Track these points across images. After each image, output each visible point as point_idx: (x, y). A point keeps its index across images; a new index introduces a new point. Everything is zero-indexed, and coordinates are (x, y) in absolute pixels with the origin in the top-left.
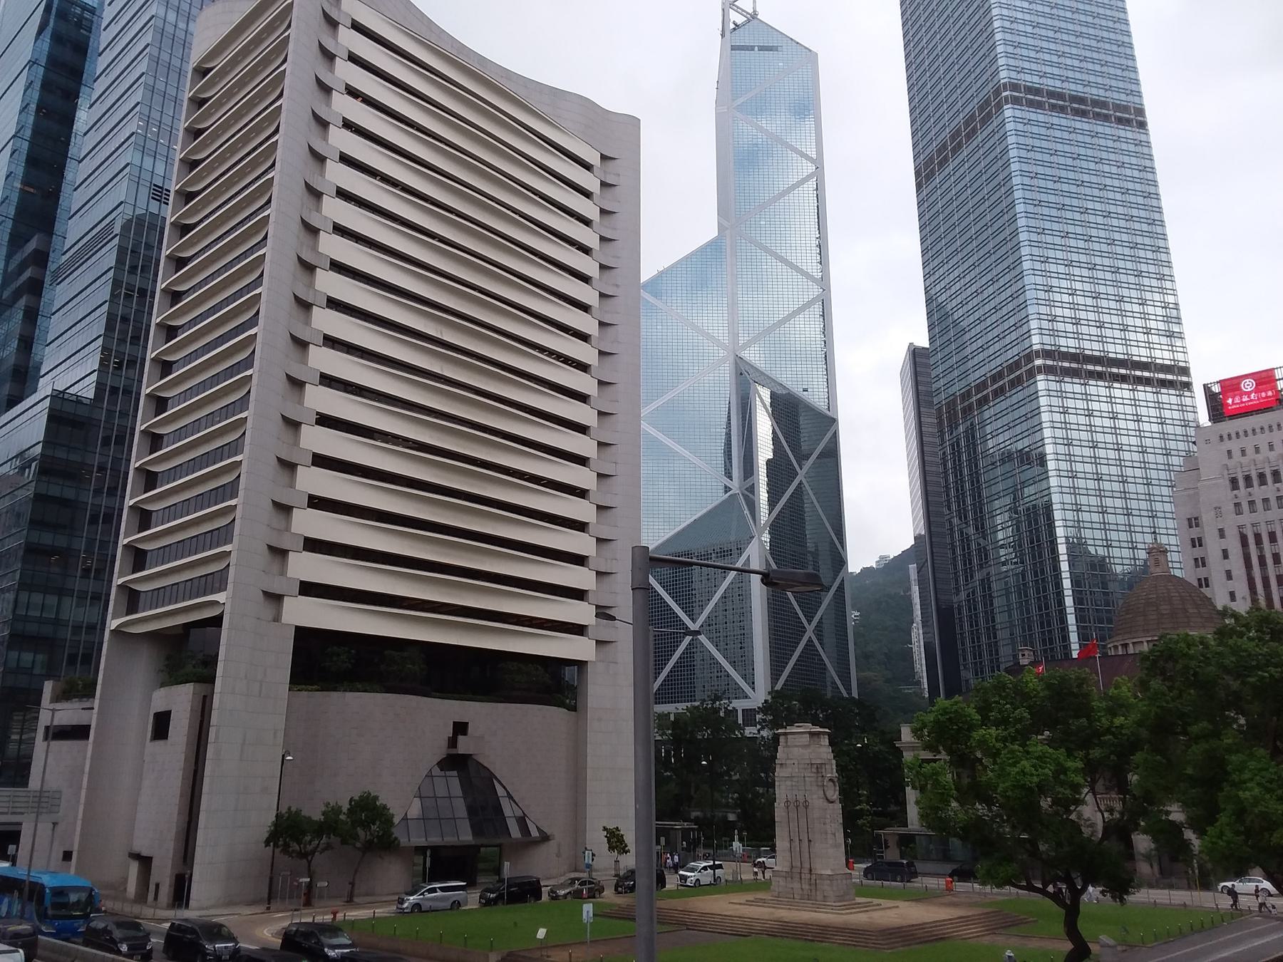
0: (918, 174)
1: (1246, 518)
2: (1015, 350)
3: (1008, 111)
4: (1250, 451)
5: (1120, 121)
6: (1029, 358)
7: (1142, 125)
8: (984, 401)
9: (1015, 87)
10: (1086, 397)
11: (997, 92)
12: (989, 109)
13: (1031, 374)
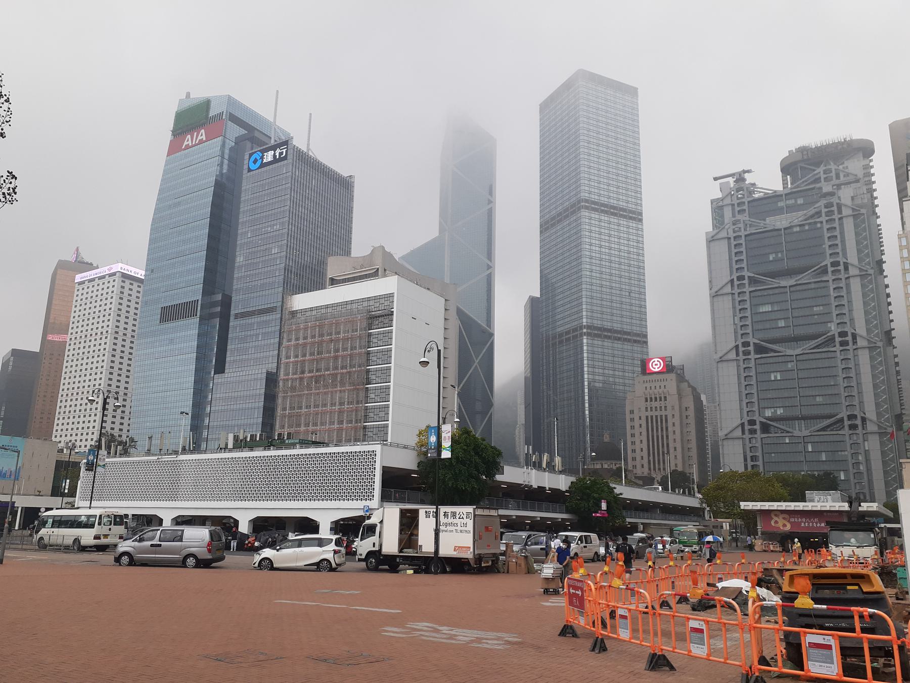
0: (541, 226)
1: (649, 414)
2: (576, 323)
3: (585, 213)
4: (653, 388)
5: (631, 218)
6: (581, 328)
7: (641, 220)
8: (561, 342)
9: (587, 201)
10: (603, 347)
11: (579, 202)
12: (575, 208)
13: (581, 335)
